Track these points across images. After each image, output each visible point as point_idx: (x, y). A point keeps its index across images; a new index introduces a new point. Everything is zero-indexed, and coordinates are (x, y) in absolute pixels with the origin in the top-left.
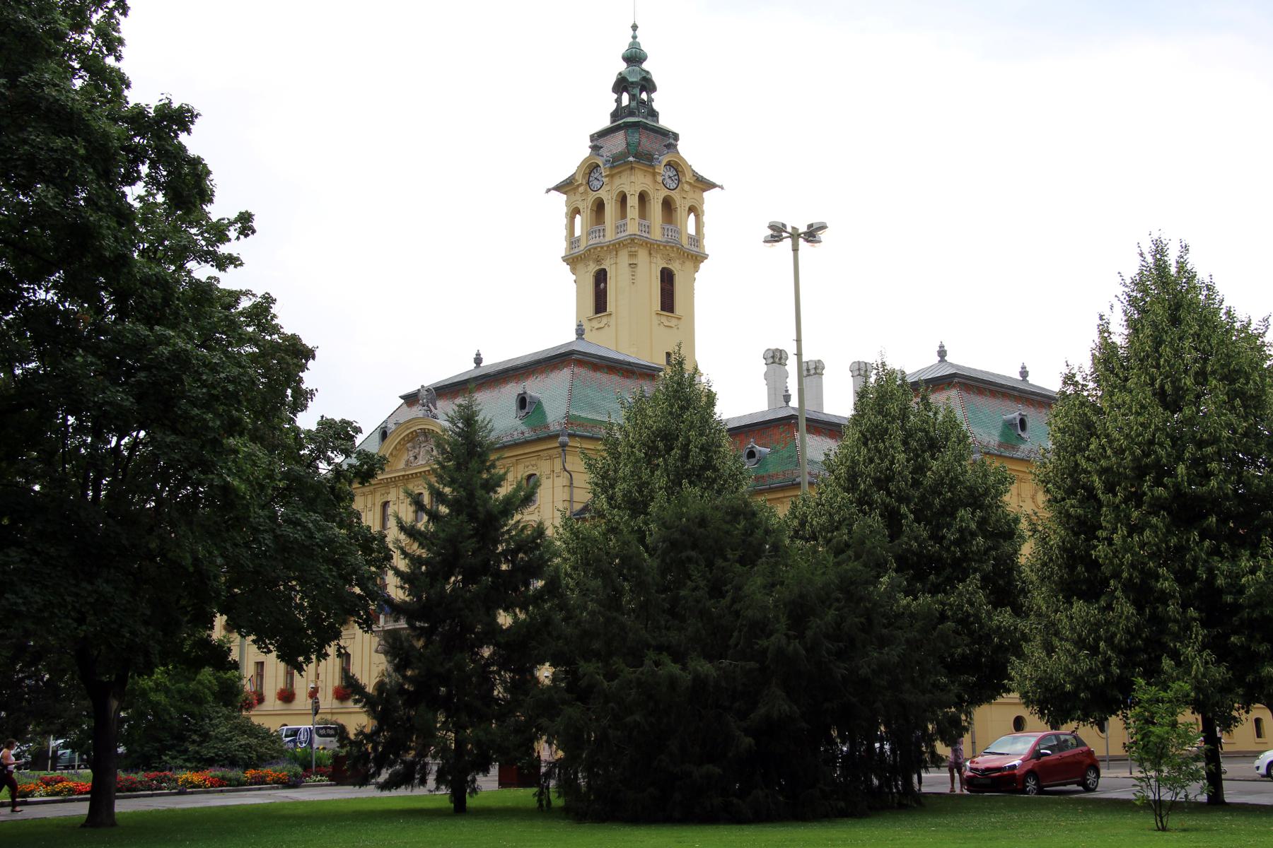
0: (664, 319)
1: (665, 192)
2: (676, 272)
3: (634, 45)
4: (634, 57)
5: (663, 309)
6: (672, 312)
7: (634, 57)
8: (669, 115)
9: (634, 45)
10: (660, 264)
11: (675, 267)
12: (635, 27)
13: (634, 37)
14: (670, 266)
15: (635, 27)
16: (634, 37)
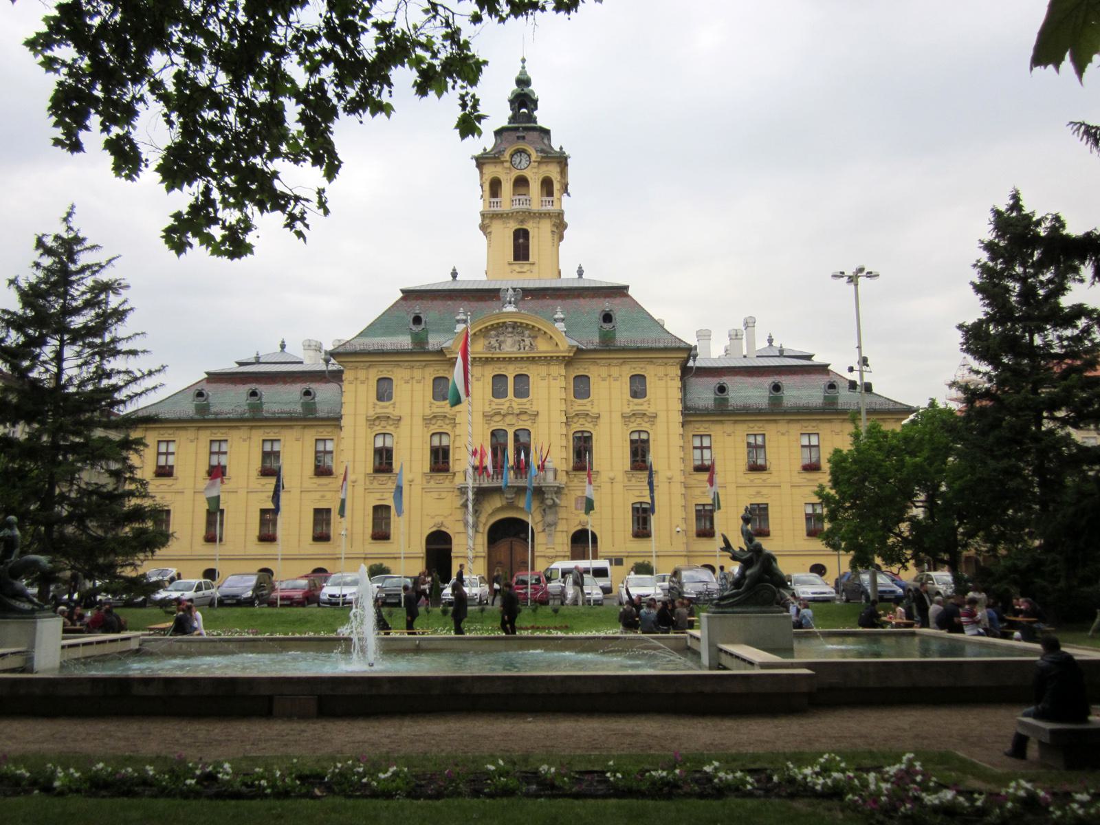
0: (517, 268)
1: (515, 174)
2: (529, 230)
3: (523, 72)
4: (523, 82)
5: (515, 260)
6: (527, 259)
7: (523, 82)
8: (543, 118)
9: (523, 72)
10: (514, 226)
11: (530, 226)
12: (523, 61)
13: (523, 68)
14: (524, 227)
15: (523, 61)
16: (523, 68)
